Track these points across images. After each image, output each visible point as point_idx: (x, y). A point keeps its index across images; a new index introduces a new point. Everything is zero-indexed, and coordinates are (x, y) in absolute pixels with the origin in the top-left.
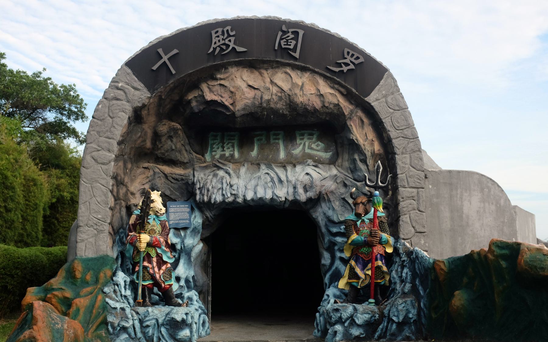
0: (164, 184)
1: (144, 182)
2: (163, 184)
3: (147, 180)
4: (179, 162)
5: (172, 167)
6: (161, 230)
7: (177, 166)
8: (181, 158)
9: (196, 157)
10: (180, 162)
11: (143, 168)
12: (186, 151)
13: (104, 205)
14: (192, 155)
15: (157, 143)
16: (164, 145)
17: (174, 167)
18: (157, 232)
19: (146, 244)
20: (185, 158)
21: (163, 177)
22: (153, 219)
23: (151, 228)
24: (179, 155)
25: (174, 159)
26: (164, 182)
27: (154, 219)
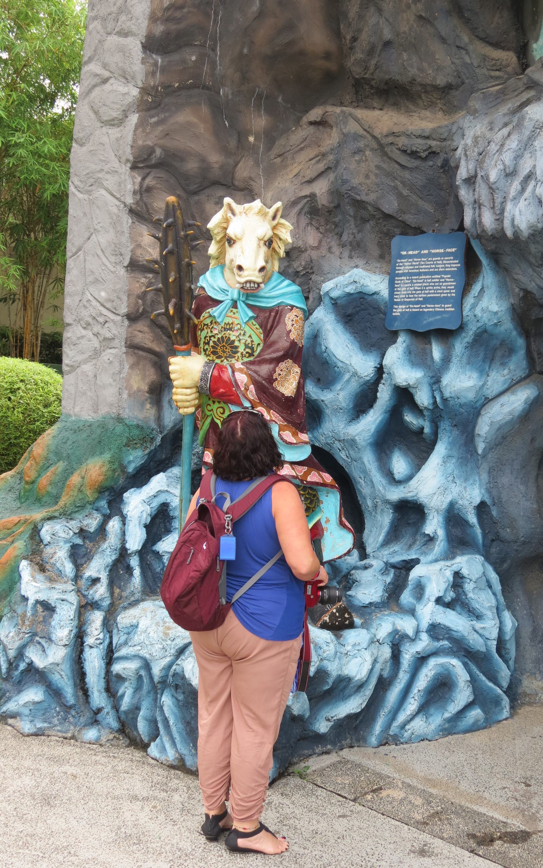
0: (376, 175)
1: (310, 174)
2: (373, 177)
3: (321, 167)
4: (419, 88)
5: (408, 111)
6: (256, 340)
7: (420, 102)
8: (421, 70)
9: (485, 58)
10: (424, 86)
11: (311, 123)
12: (443, 40)
13: (113, 259)
14: (467, 53)
15: (342, 26)
16: (360, 31)
17: (412, 107)
18: (241, 349)
19: (194, 390)
20: (439, 69)
21: (372, 150)
22: (228, 302)
23: (220, 336)
24: (415, 59)
25: (398, 77)
26: (378, 167)
27: (235, 305)
